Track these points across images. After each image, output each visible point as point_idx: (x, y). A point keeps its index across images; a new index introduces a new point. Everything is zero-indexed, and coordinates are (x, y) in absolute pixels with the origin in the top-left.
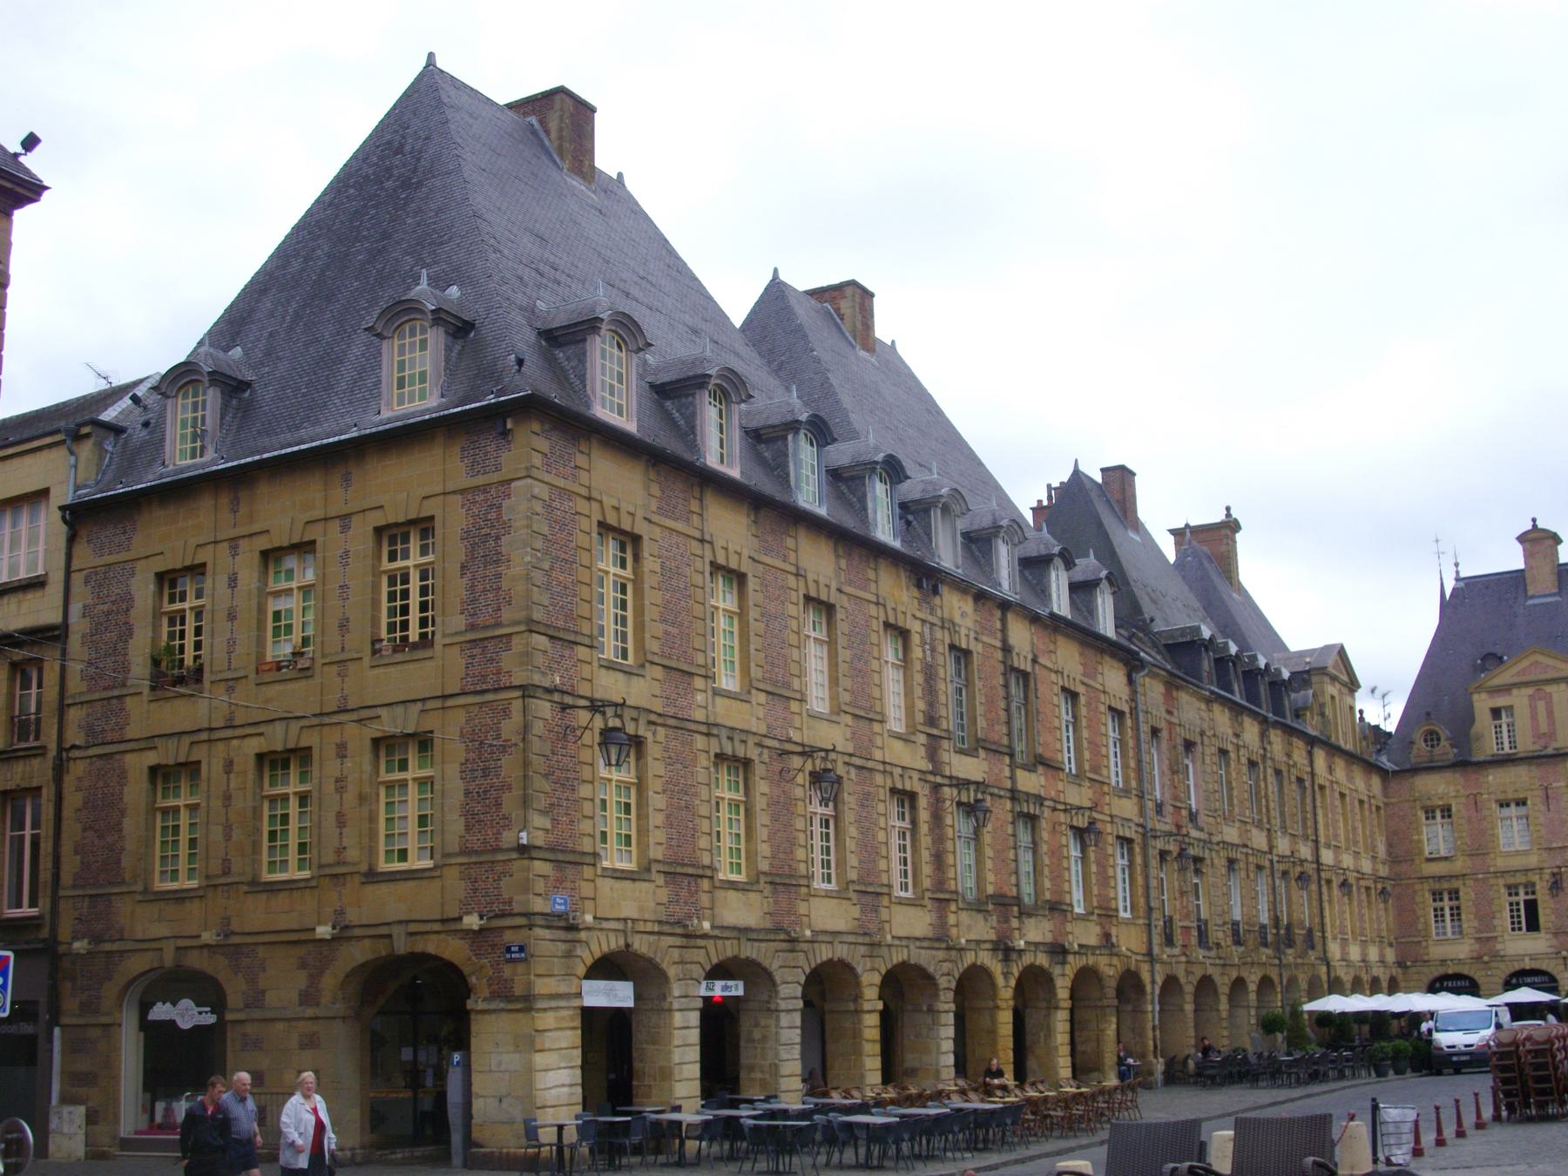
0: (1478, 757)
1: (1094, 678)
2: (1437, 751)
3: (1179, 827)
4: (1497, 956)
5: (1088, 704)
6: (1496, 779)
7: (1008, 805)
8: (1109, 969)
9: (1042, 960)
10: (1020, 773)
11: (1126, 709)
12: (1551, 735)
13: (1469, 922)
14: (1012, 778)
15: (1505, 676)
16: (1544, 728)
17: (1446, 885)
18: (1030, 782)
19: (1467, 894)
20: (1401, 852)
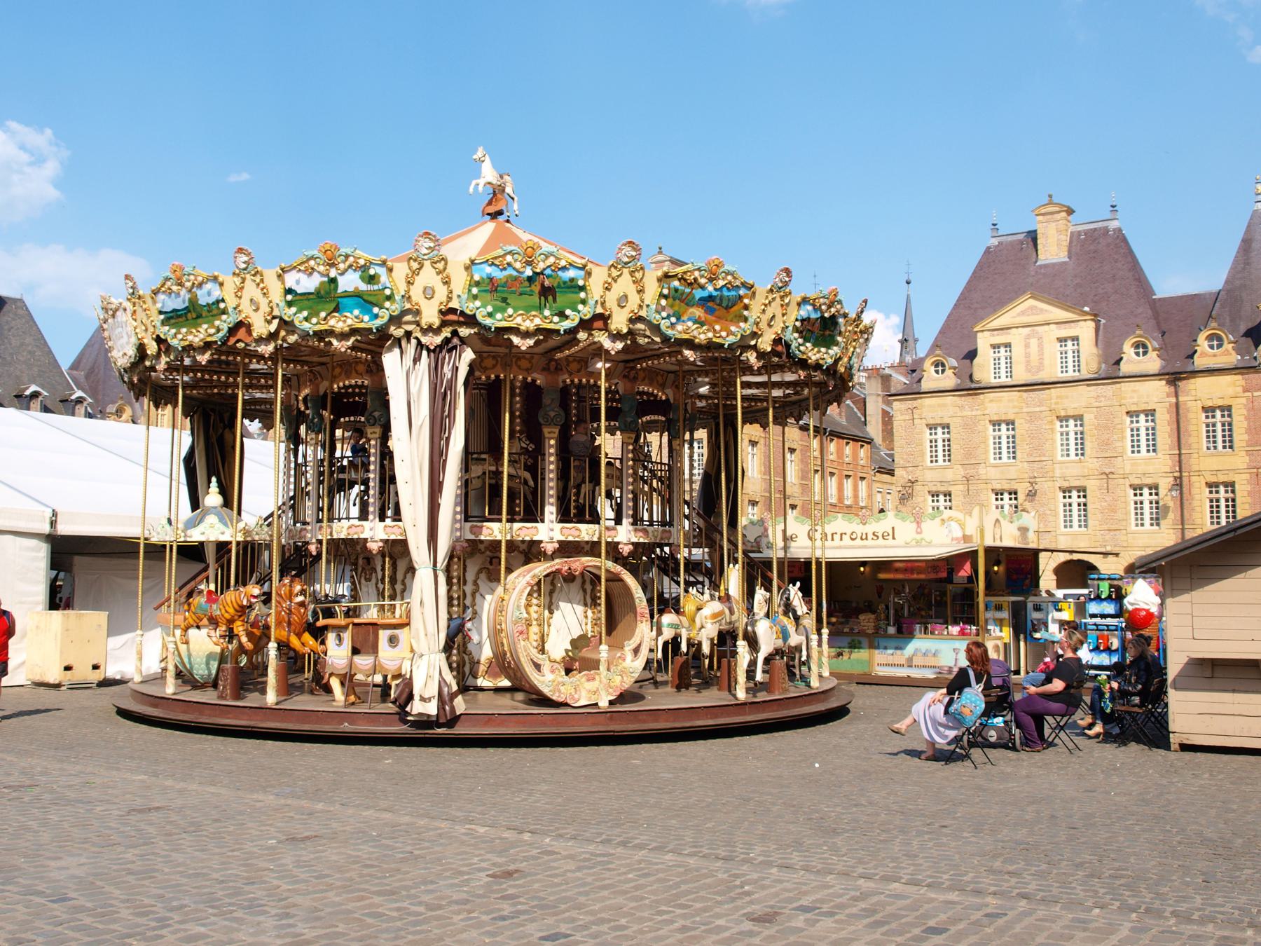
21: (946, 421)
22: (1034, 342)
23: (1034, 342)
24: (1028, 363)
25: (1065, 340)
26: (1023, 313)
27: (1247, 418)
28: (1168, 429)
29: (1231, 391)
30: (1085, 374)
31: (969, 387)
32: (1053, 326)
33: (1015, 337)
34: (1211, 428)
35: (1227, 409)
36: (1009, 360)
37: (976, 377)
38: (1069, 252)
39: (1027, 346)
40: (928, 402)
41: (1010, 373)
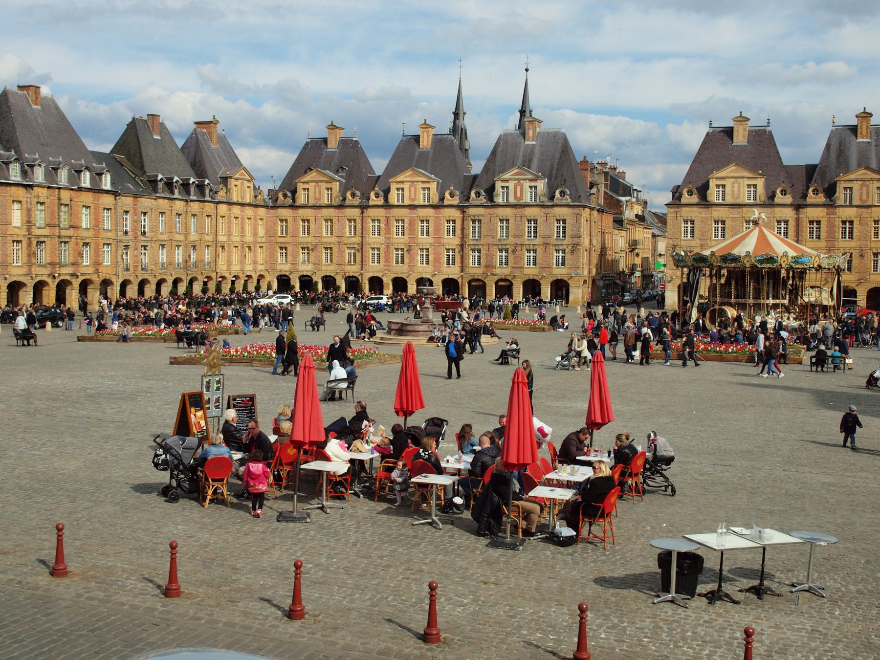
0: (297, 204)
1: (98, 201)
2: (286, 200)
3: (136, 238)
4: (297, 270)
5: (95, 209)
6: (301, 212)
7: (57, 239)
8: (97, 280)
9: (68, 278)
10: (62, 231)
11: (113, 207)
12: (319, 199)
13: (290, 258)
14: (60, 232)
15: (307, 178)
16: (317, 197)
17: (283, 246)
18: (63, 233)
19: (290, 249)
20: (270, 233)
21: (693, 219)
22: (736, 185)
23: (736, 185)
24: (733, 195)
25: (750, 185)
26: (731, 172)
27: (827, 226)
28: (794, 229)
29: (821, 214)
30: (758, 202)
31: (704, 202)
32: (745, 179)
33: (728, 183)
34: (811, 229)
35: (818, 222)
36: (724, 192)
37: (709, 199)
38: (748, 140)
39: (733, 187)
40: (684, 209)
41: (723, 199)
